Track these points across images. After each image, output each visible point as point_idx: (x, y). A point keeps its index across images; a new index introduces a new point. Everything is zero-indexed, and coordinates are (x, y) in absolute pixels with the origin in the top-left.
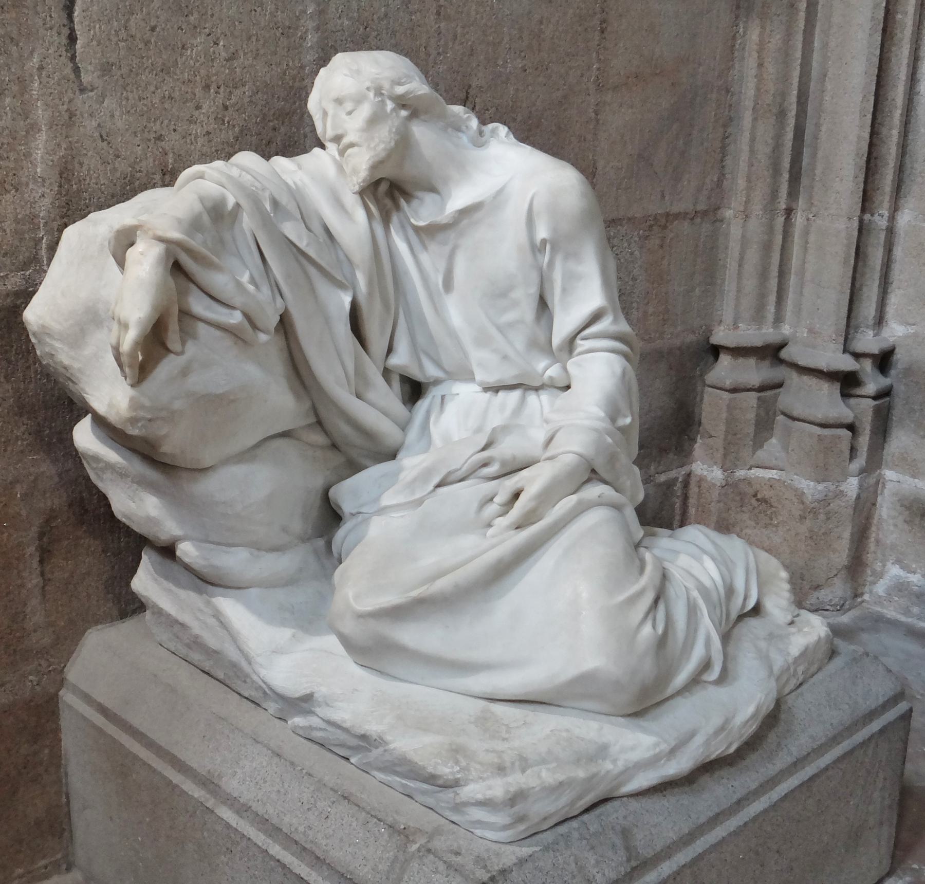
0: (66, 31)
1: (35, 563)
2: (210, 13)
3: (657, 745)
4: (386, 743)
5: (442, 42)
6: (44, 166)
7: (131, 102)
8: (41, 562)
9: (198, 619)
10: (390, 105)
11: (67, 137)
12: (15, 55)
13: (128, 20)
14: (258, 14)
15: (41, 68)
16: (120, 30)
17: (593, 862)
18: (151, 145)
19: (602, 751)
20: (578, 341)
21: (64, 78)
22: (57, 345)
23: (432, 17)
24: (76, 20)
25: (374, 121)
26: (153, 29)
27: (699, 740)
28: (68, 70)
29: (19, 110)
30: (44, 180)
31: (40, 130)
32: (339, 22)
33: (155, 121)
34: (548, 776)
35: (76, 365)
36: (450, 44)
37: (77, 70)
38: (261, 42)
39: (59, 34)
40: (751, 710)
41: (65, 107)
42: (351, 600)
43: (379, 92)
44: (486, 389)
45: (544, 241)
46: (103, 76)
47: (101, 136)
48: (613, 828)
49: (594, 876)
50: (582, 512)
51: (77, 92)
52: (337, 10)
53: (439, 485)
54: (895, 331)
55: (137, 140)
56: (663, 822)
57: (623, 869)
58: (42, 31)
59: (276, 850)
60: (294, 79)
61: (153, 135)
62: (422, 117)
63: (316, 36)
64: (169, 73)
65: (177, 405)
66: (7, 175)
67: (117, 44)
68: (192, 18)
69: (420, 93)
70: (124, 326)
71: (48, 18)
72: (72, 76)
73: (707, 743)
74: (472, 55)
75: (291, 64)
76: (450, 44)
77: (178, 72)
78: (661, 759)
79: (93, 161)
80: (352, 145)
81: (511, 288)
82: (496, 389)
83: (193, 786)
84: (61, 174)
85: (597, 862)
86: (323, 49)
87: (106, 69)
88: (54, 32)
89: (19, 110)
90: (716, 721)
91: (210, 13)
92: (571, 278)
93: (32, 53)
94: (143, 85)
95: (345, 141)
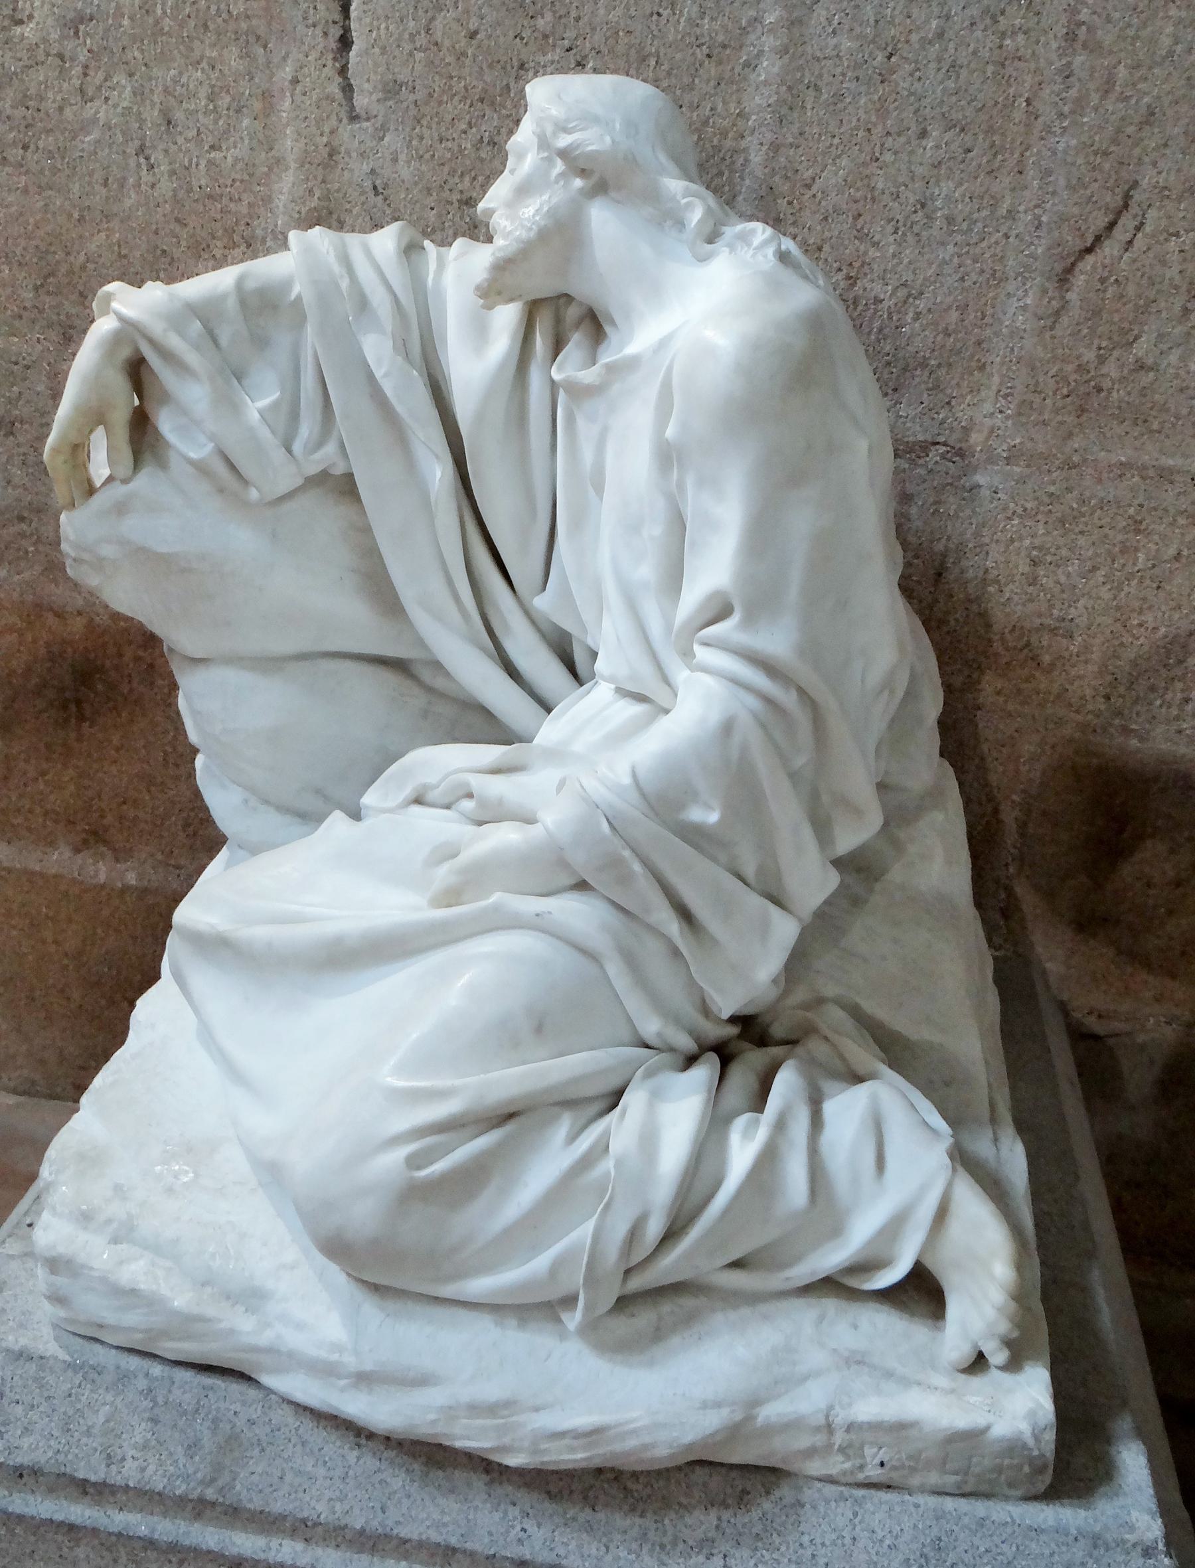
0: (336, 32)
2: (573, 14)
3: (337, 1347)
5: (1073, 93)
6: (286, 218)
7: (427, 141)
10: (559, 166)
11: (324, 181)
12: (261, 60)
13: (433, 19)
14: (663, 20)
15: (295, 81)
16: (419, 33)
17: (139, 1439)
18: (453, 209)
19: (252, 1297)
21: (327, 98)
23: (1054, 45)
24: (353, 14)
26: (473, 35)
27: (435, 1397)
28: (334, 89)
29: (261, 136)
31: (287, 169)
32: (833, 42)
33: (462, 175)
34: (136, 1271)
36: (1095, 98)
37: (348, 89)
38: (665, 67)
39: (326, 34)
40: (582, 1420)
41: (325, 139)
46: (385, 99)
47: (375, 188)
48: (215, 1421)
49: (124, 1459)
50: (514, 928)
51: (345, 121)
52: (829, 21)
55: (430, 201)
56: (330, 1484)
57: (184, 1487)
58: (300, 28)
60: (724, 134)
61: (455, 197)
62: (613, 194)
63: (779, 63)
64: (493, 104)
65: (107, 551)
66: (237, 223)
67: (411, 54)
68: (540, 22)
69: (590, 148)
71: (312, 11)
73: (450, 1412)
74: (1147, 123)
75: (720, 106)
76: (1095, 98)
77: (509, 104)
78: (339, 1377)
79: (360, 220)
85: (145, 1447)
86: (790, 88)
87: (392, 89)
88: (319, 31)
89: (261, 136)
90: (491, 1391)
91: (573, 14)
93: (285, 59)
94: (448, 118)
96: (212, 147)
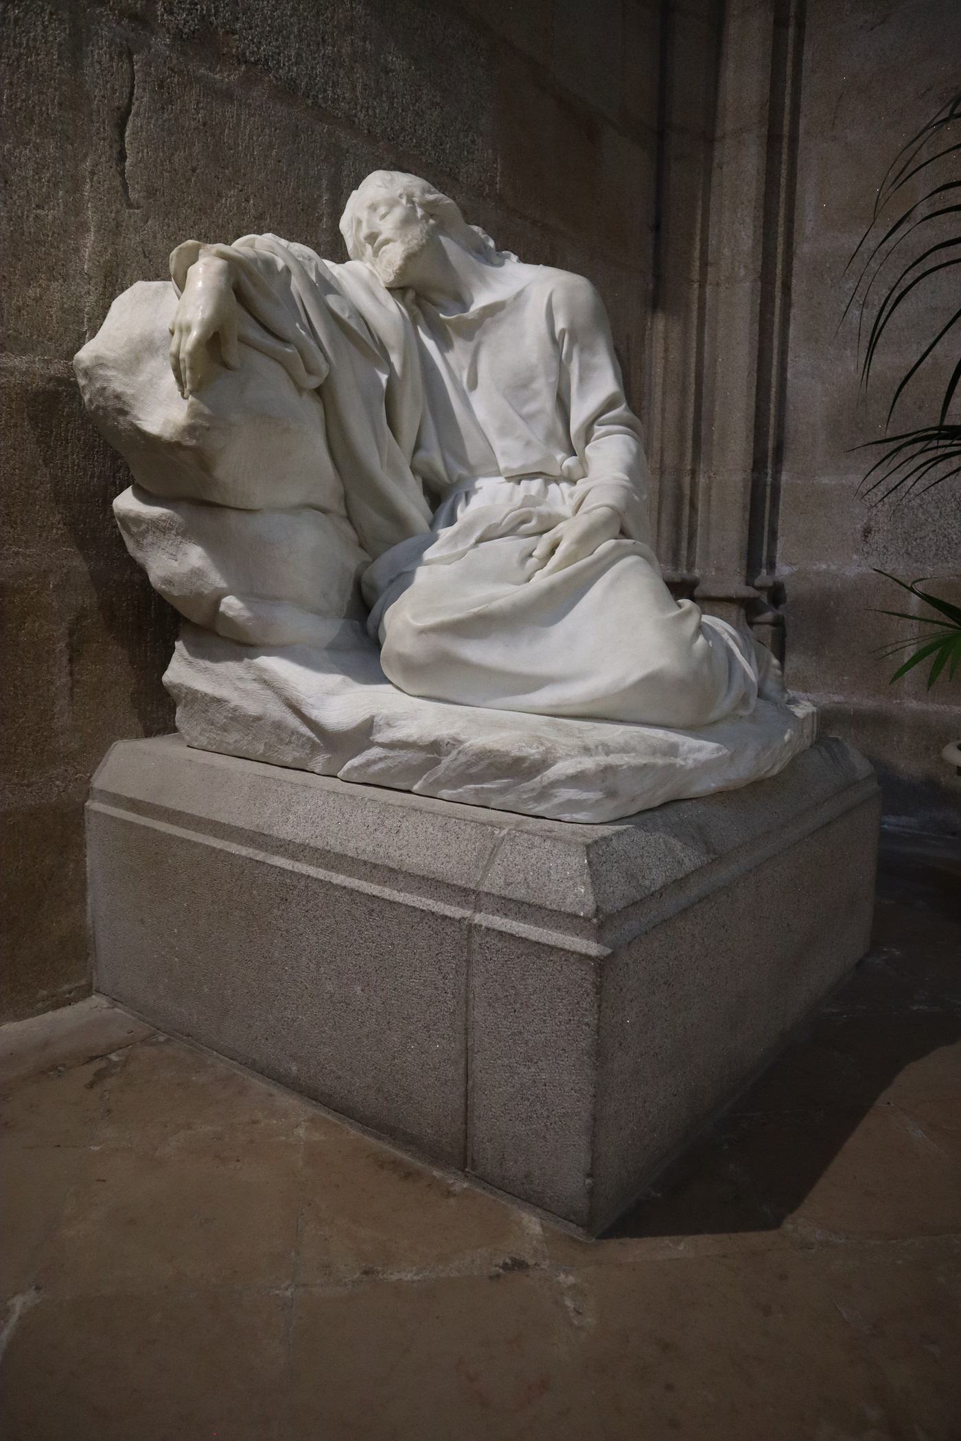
1: (65, 660)
3: (718, 750)
4: (461, 742)
8: (71, 660)
9: (236, 689)
10: (420, 212)
15: (93, 173)
19: (673, 750)
20: (596, 427)
22: (110, 373)
24: (127, 140)
25: (407, 221)
26: (194, 170)
28: (117, 182)
30: (90, 278)
35: (130, 391)
37: (125, 186)
42: (412, 621)
43: (410, 200)
44: (509, 479)
45: (563, 332)
53: (480, 541)
54: (783, 571)
59: (339, 879)
70: (188, 329)
72: (120, 189)
80: (387, 242)
81: (532, 379)
82: (517, 478)
83: (239, 847)
84: (106, 277)
87: (151, 192)
92: (586, 371)
93: (86, 155)
95: (381, 238)
96: (38, 207)
